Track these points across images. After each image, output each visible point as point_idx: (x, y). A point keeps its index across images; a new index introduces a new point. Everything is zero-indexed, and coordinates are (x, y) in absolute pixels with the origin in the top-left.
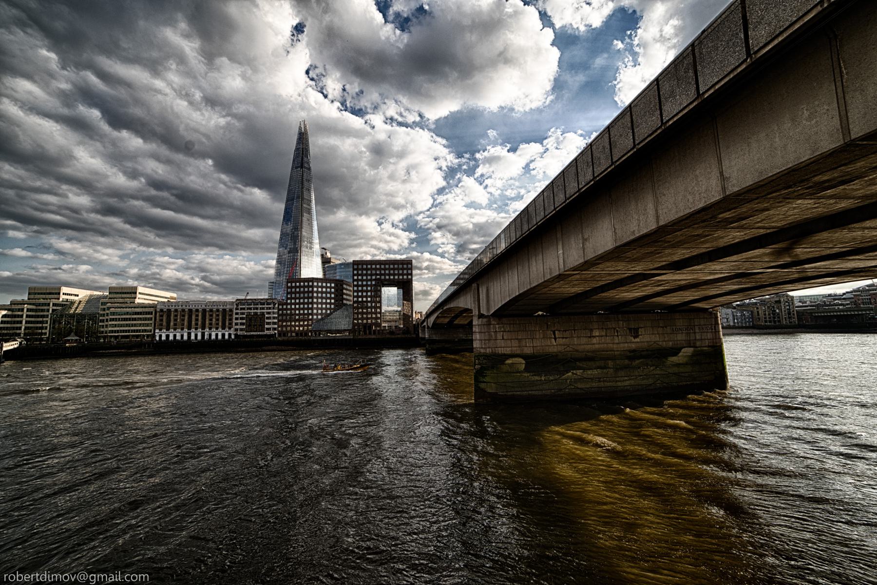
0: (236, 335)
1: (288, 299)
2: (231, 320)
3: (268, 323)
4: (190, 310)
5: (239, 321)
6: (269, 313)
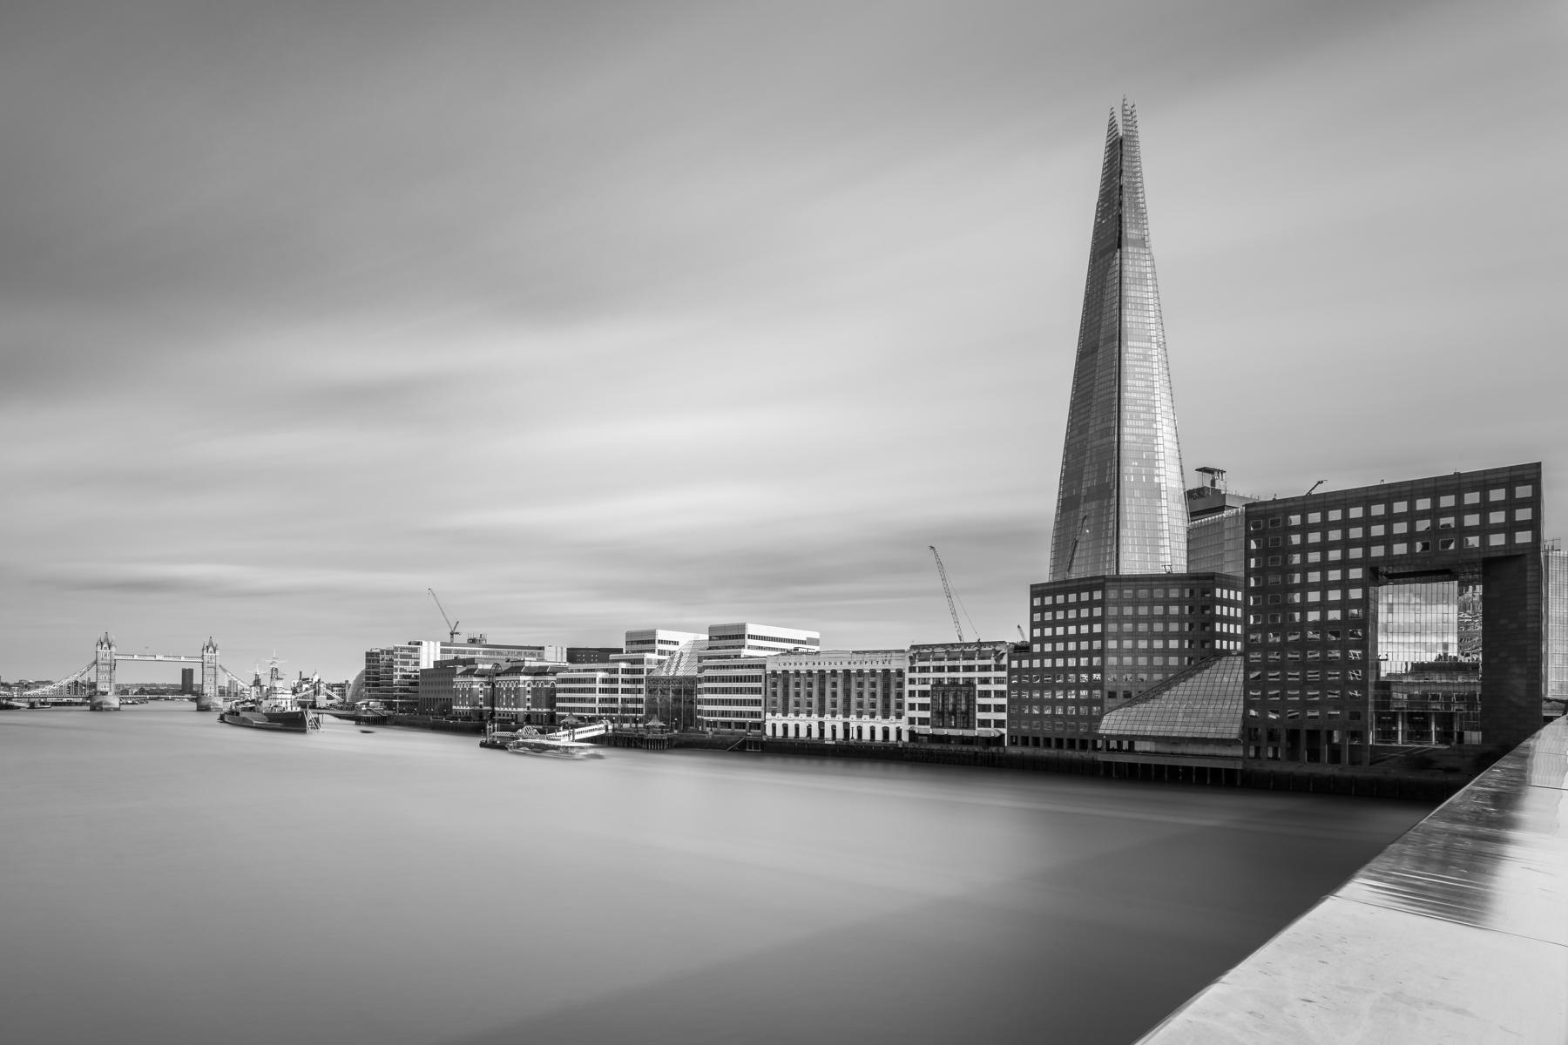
0: (912, 733)
2: (900, 695)
3: (985, 708)
4: (822, 672)
5: (918, 700)
6: (985, 681)
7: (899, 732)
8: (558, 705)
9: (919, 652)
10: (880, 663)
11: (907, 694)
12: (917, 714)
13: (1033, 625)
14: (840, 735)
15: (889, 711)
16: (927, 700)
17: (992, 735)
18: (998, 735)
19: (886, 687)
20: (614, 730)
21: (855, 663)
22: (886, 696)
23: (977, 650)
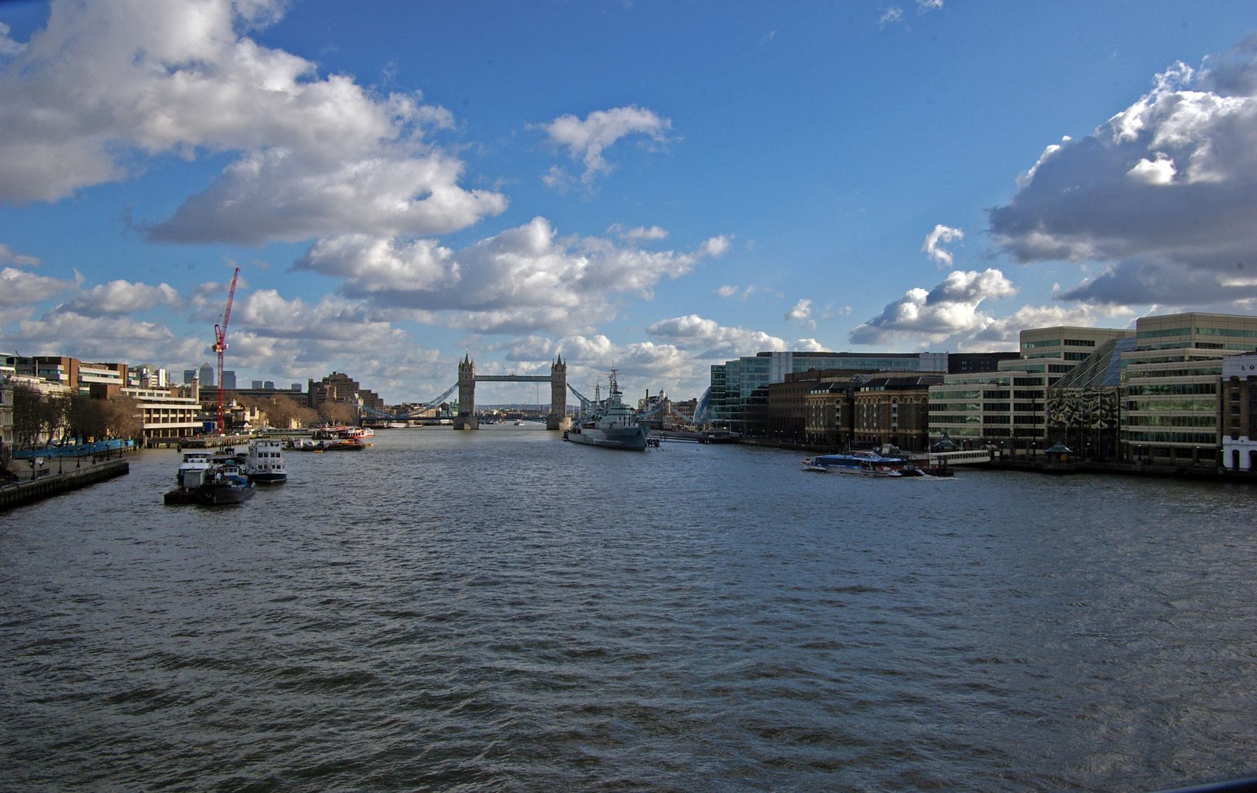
20: (1002, 456)
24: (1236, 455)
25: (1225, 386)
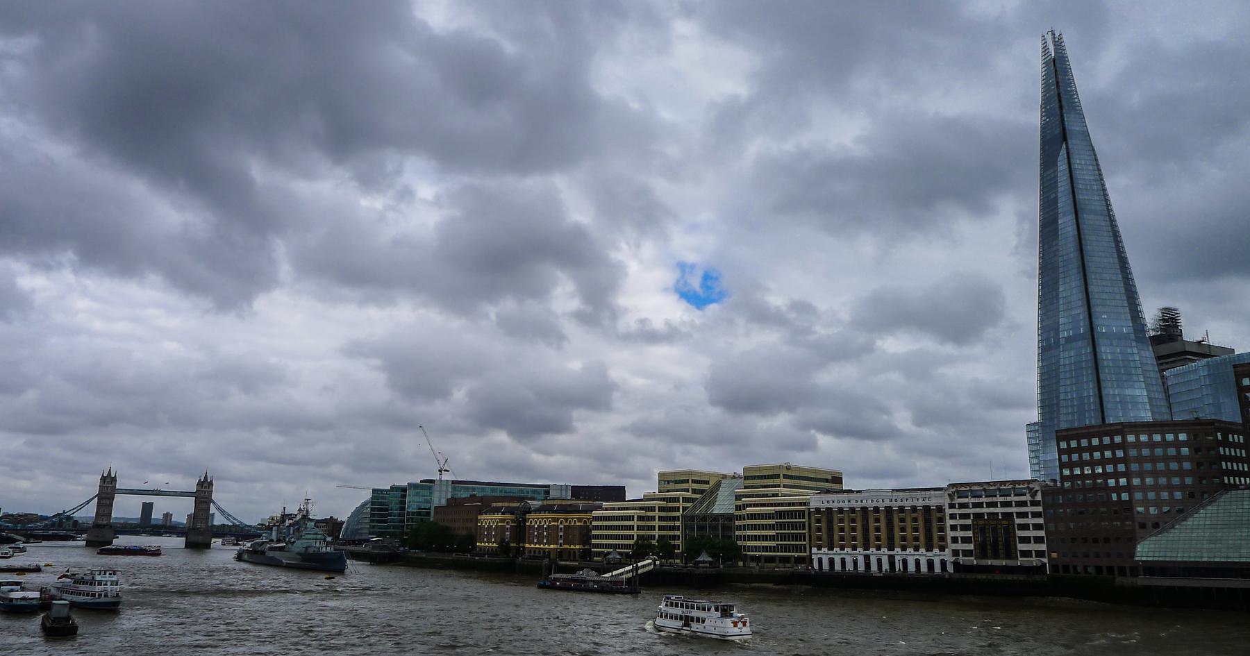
0: (956, 564)
1: (1063, 478)
2: (942, 529)
3: (1025, 540)
4: (864, 510)
5: (960, 534)
6: (1023, 515)
7: (943, 563)
8: (594, 541)
9: (957, 490)
10: (921, 501)
11: (948, 529)
12: (960, 546)
13: (1062, 466)
14: (885, 566)
15: (932, 544)
16: (970, 534)
17: (1035, 565)
18: (1040, 564)
19: (928, 521)
20: (661, 565)
21: (896, 500)
22: (928, 531)
23: (1012, 488)
24: (820, 560)
25: (812, 514)
